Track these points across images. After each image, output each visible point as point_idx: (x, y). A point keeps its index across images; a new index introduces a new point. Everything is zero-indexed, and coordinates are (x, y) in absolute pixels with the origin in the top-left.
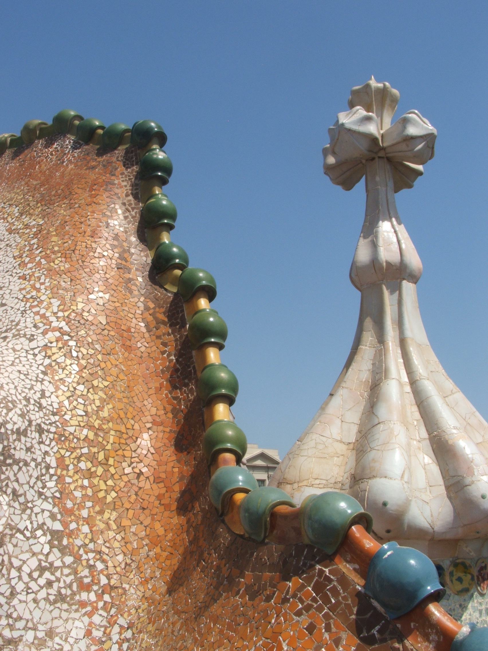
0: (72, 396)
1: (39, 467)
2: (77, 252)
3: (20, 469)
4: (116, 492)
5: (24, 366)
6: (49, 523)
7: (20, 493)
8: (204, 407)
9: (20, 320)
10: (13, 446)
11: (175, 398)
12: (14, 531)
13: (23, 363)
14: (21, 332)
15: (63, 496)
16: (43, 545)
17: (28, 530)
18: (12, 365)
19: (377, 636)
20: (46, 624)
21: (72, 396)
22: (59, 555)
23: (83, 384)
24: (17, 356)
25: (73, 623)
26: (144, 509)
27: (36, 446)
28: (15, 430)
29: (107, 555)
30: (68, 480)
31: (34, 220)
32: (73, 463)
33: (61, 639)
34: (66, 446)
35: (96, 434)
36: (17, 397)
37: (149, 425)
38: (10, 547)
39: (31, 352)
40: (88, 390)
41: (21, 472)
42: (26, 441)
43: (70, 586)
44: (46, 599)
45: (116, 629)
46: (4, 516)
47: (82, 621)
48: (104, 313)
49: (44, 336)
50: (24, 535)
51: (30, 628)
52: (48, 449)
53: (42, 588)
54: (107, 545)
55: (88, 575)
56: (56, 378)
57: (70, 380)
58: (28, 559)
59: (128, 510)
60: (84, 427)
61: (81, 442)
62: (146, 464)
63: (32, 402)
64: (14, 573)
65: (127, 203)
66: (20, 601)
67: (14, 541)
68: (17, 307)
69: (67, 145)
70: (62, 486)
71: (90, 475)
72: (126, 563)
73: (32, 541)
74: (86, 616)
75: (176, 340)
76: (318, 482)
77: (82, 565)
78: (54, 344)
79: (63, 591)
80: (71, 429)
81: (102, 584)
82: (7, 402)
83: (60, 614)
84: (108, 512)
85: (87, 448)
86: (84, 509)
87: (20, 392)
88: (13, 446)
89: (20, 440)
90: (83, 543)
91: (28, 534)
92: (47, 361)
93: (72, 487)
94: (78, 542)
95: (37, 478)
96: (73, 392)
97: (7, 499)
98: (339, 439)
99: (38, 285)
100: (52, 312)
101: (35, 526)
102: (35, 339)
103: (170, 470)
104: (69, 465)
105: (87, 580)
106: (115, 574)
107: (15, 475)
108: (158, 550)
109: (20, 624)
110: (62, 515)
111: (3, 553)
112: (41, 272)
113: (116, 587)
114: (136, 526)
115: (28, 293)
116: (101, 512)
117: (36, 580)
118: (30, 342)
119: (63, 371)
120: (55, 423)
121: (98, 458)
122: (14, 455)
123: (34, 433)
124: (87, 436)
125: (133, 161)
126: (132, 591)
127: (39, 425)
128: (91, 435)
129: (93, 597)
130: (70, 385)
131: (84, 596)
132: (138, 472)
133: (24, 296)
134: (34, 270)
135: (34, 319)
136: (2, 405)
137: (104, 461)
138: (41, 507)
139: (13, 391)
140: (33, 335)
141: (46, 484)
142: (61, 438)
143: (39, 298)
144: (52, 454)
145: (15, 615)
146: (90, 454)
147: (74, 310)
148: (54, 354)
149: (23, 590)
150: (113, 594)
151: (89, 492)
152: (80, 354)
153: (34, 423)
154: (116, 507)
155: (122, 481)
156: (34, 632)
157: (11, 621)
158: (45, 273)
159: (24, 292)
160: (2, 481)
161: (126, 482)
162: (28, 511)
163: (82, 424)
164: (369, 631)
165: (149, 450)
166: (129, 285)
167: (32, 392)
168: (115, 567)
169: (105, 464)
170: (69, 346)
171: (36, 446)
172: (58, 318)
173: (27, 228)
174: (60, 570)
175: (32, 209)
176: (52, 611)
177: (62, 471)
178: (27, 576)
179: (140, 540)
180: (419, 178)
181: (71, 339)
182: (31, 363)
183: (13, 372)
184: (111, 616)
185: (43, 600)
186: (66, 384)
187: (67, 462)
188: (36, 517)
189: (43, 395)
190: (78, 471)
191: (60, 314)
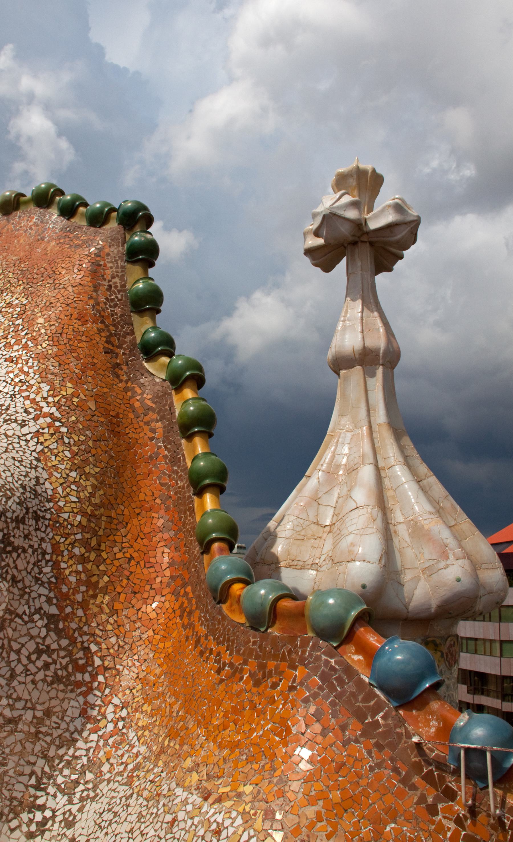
0: (65, 482)
1: (36, 553)
2: (64, 335)
3: (19, 556)
5: (17, 452)
6: (46, 607)
7: (18, 579)
9: (9, 405)
10: (12, 534)
12: (13, 616)
13: (17, 449)
14: (12, 417)
15: (59, 580)
16: (40, 628)
17: (26, 615)
18: (6, 451)
19: (381, 721)
20: (44, 703)
21: (65, 482)
22: (55, 638)
23: (76, 471)
24: (9, 442)
25: (69, 703)
26: (135, 593)
27: (33, 533)
28: (14, 518)
30: (63, 565)
31: (17, 299)
32: (67, 549)
33: (58, 717)
35: (89, 521)
36: (14, 485)
37: (137, 511)
38: (10, 631)
39: (24, 438)
40: (81, 476)
41: (19, 559)
42: (24, 529)
43: (66, 668)
44: (44, 680)
45: (111, 708)
46: (4, 602)
47: (77, 701)
48: (93, 399)
49: (35, 422)
50: (23, 620)
51: (29, 708)
52: (43, 535)
53: (39, 669)
55: (83, 657)
56: (49, 464)
57: (63, 467)
58: (26, 643)
60: (77, 513)
61: (75, 528)
62: (137, 549)
63: (28, 489)
64: (13, 656)
65: (113, 286)
66: (20, 683)
67: (13, 625)
68: (6, 390)
69: (47, 219)
71: (83, 560)
72: (119, 645)
73: (30, 625)
74: (81, 696)
75: (164, 427)
76: (295, 563)
77: (77, 647)
78: (46, 430)
79: (60, 673)
80: (66, 516)
81: (96, 666)
82: (5, 491)
83: (57, 694)
85: (80, 534)
86: (78, 593)
87: (17, 479)
88: (12, 534)
89: (18, 528)
90: (77, 626)
91: (26, 618)
92: (40, 448)
93: (67, 572)
94: (73, 626)
95: (34, 564)
97: (7, 585)
98: (316, 521)
99: (26, 369)
100: (42, 397)
101: (33, 610)
102: (26, 425)
104: (63, 551)
105: (81, 662)
106: (108, 655)
107: (14, 562)
109: (20, 705)
110: (58, 600)
111: (3, 637)
112: (28, 355)
113: (110, 669)
115: (16, 376)
116: (95, 596)
117: (34, 663)
118: (22, 428)
120: (49, 509)
121: (90, 544)
122: (13, 542)
123: (31, 520)
124: (80, 522)
125: (119, 242)
127: (35, 512)
128: (85, 522)
129: (87, 677)
130: (63, 471)
131: (79, 676)
132: (129, 557)
133: (12, 380)
134: (20, 353)
135: (24, 404)
136: (1, 494)
138: (38, 592)
139: (10, 479)
140: (24, 421)
143: (28, 382)
144: (48, 540)
145: (14, 696)
147: (63, 396)
148: (46, 440)
149: (22, 673)
150: (107, 675)
151: (83, 576)
152: (71, 440)
153: (31, 511)
154: (109, 591)
156: (32, 712)
157: (11, 702)
158: (33, 356)
159: (12, 375)
160: (3, 568)
162: (26, 597)
163: (75, 511)
164: (373, 717)
166: (117, 370)
167: (28, 479)
169: (98, 549)
170: (60, 432)
171: (33, 533)
172: (48, 403)
173: (10, 307)
174: (56, 653)
175: (14, 286)
176: (49, 691)
177: (57, 557)
178: (26, 659)
179: (132, 623)
180: (399, 261)
181: (62, 426)
182: (24, 449)
183: (8, 459)
184: (106, 696)
185: (41, 682)
186: (60, 471)
187: (62, 549)
188: (34, 602)
189: (38, 483)
190: (73, 557)
191: (50, 399)
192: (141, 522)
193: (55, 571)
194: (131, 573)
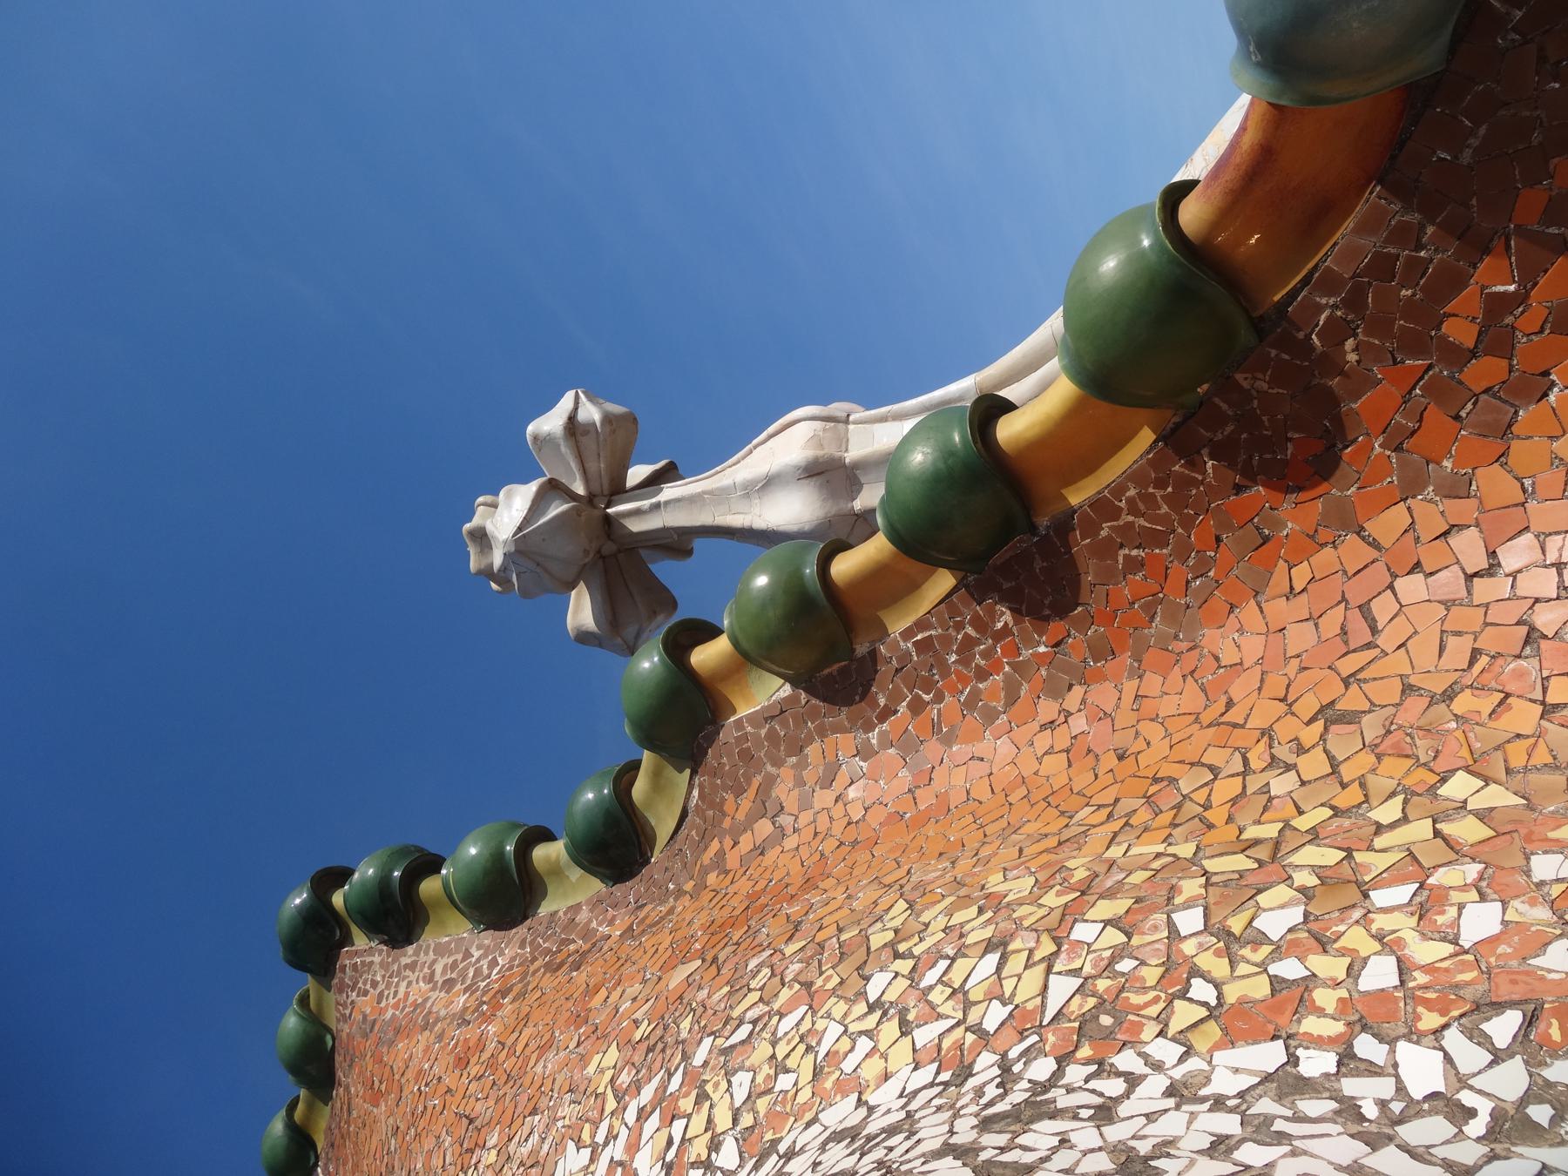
0: (903, 1013)
8: (1033, 529)
11: (1012, 699)
15: (1504, 992)
30: (1380, 974)
34: (1156, 1000)
37: (1110, 761)
52: (1155, 1085)
60: (1058, 942)
70: (1427, 1003)
75: (822, 733)
80: (1060, 988)
93: (1427, 952)
96: (885, 1013)
103: (1305, 595)
119: (787, 1071)
130: (853, 1028)
141: (1417, 1092)
142: (1100, 1030)
144: (1194, 1064)
146: (1211, 900)
161: (1379, 757)
163: (1048, 947)
177: (1320, 1012)
193: (1430, 1020)
194: (1408, 689)
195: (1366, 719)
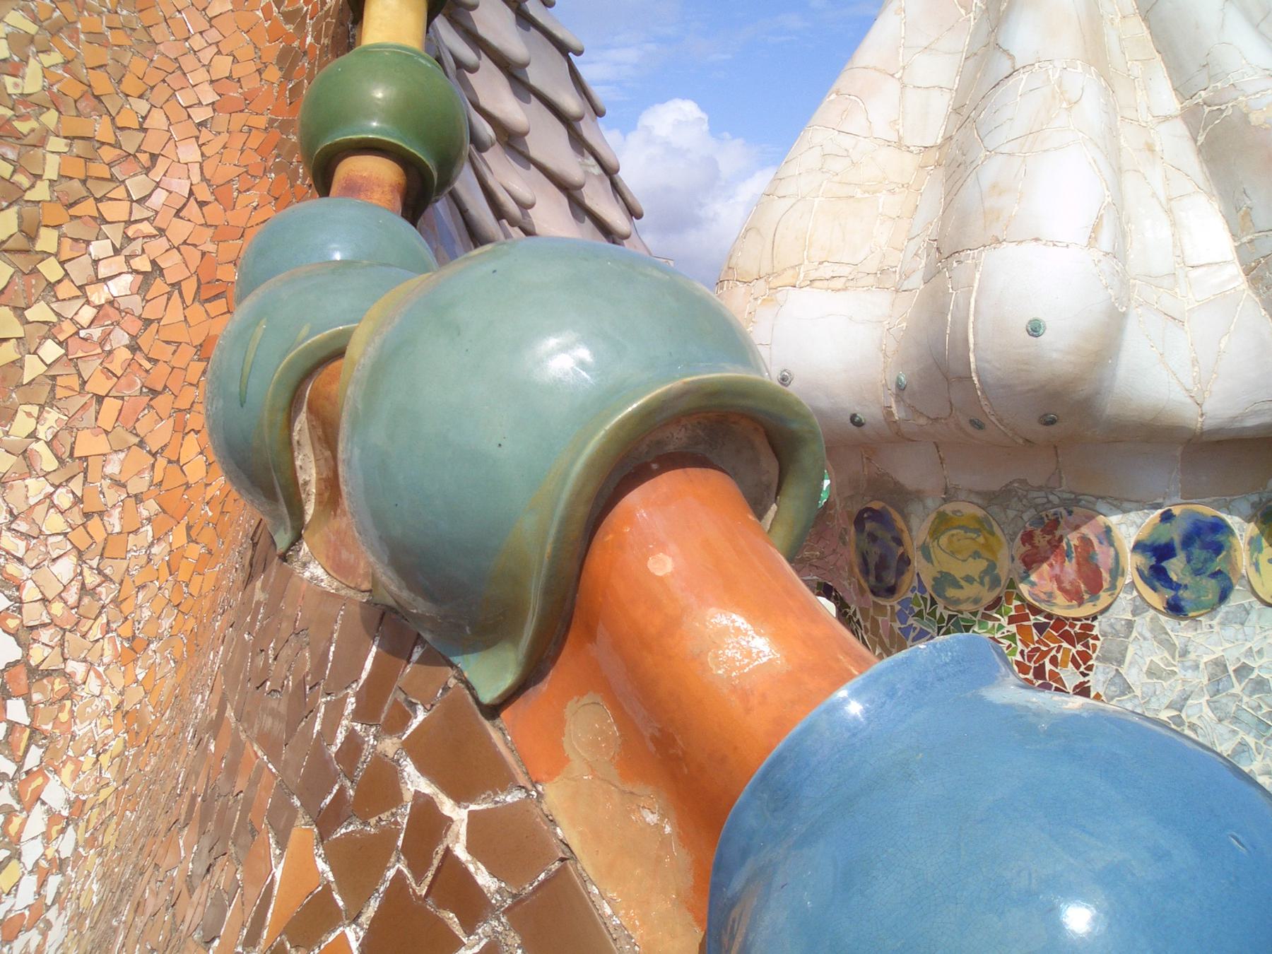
4: (60, 344)
26: (154, 393)
29: (20, 560)
54: (22, 526)
59: (100, 399)
84: (29, 414)
106: (44, 625)
108: (178, 537)
113: (49, 673)
114: (122, 455)
126: (93, 685)
132: (147, 267)
137: (20, 242)
150: (36, 697)
154: (60, 393)
155: (88, 302)
161: (100, 307)
165: (191, 193)
168: (44, 600)
192: (208, 150)
195: (138, 298)
